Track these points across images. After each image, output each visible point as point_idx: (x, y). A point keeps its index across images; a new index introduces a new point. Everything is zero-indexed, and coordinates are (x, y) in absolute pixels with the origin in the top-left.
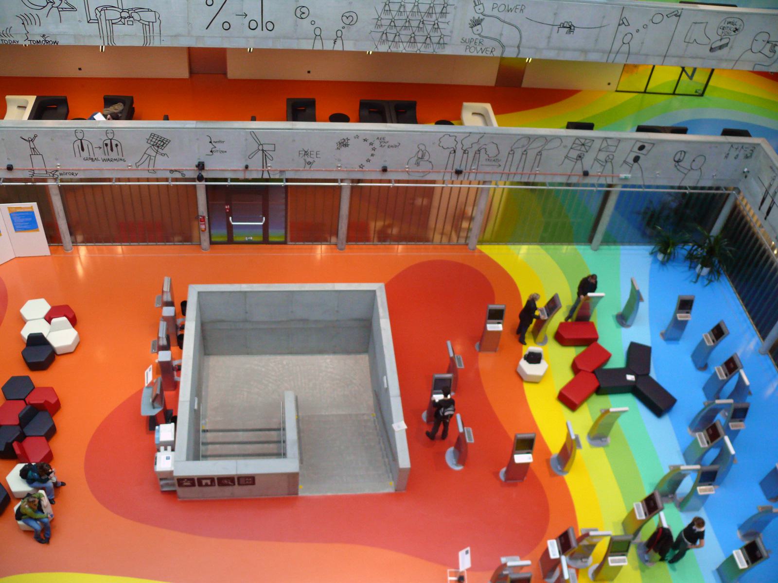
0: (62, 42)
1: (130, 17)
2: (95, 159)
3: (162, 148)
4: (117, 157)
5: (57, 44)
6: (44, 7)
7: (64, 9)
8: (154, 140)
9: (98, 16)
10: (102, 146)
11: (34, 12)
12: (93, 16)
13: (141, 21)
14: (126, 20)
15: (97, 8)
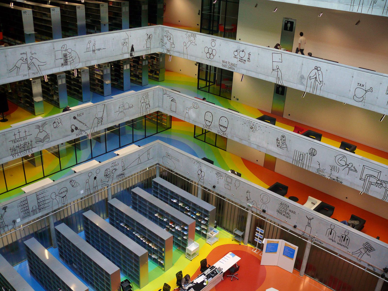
0: (344, 183)
1: (381, 184)
2: (334, 241)
3: (369, 252)
4: (345, 245)
5: (342, 183)
6: (343, 166)
7: (352, 170)
8: (367, 246)
9: (366, 178)
10: (340, 237)
11: (338, 166)
12: (363, 177)
13: (386, 188)
14: (378, 185)
15: (367, 175)
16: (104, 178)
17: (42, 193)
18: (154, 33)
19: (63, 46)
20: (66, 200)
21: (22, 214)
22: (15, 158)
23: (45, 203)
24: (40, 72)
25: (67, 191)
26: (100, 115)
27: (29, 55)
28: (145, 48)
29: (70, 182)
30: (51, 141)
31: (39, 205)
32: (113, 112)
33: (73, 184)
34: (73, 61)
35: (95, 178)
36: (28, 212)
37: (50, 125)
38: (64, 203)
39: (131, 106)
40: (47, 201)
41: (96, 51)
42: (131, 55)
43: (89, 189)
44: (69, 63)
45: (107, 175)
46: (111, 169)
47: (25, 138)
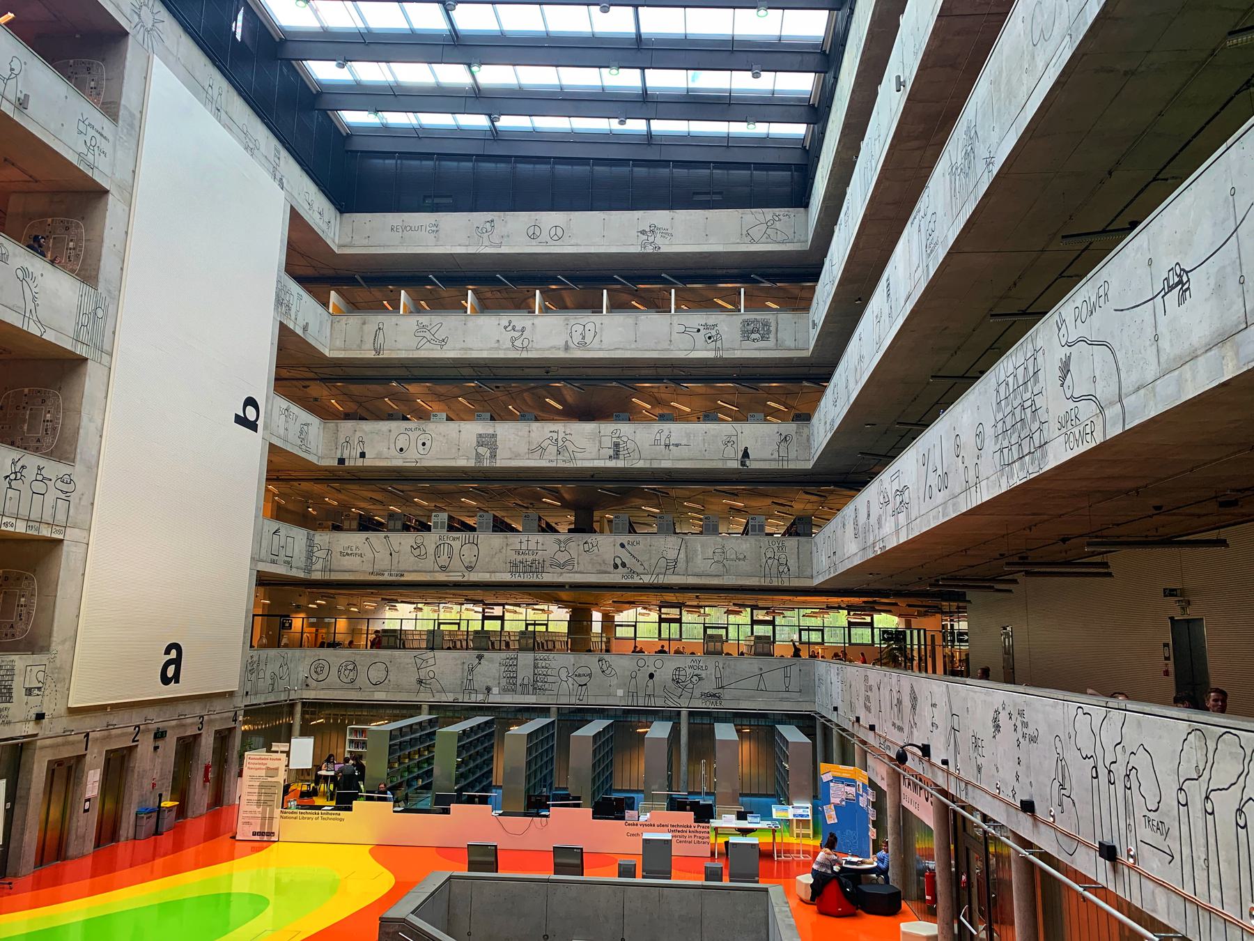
16: (670, 684)
17: (545, 660)
18: (796, 433)
19: (615, 431)
20: (586, 694)
21: (504, 682)
22: (513, 579)
23: (546, 680)
24: (574, 461)
25: (590, 675)
26: (672, 555)
27: (561, 435)
28: (776, 456)
29: (599, 661)
30: (576, 572)
31: (535, 679)
32: (700, 557)
33: (604, 668)
34: (628, 455)
35: (651, 676)
36: (514, 684)
37: (579, 545)
38: (581, 698)
39: (742, 557)
40: (550, 679)
41: (671, 447)
42: (743, 464)
43: (635, 694)
44: (622, 457)
45: (678, 682)
46: (689, 671)
47: (535, 552)
